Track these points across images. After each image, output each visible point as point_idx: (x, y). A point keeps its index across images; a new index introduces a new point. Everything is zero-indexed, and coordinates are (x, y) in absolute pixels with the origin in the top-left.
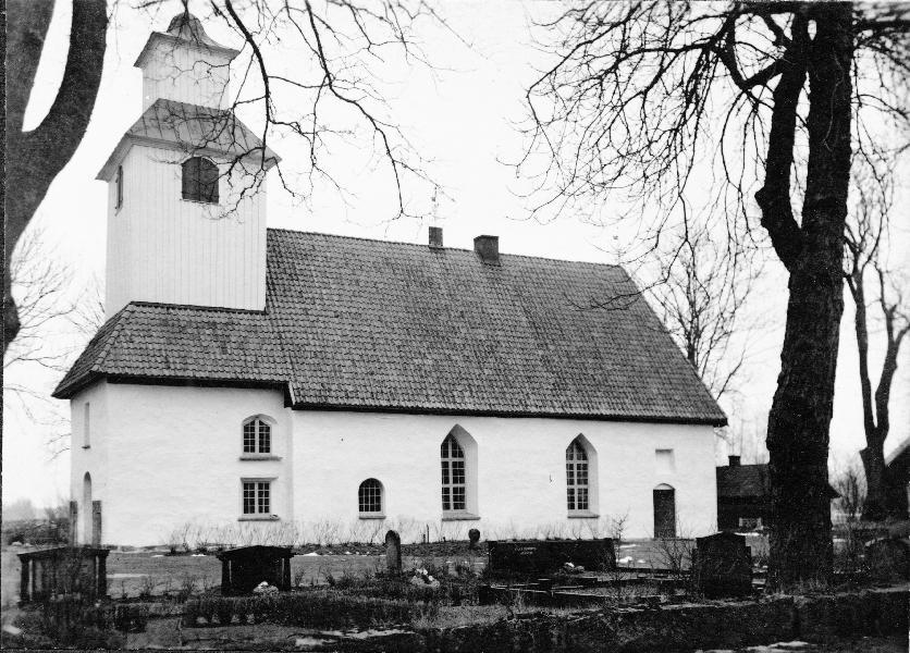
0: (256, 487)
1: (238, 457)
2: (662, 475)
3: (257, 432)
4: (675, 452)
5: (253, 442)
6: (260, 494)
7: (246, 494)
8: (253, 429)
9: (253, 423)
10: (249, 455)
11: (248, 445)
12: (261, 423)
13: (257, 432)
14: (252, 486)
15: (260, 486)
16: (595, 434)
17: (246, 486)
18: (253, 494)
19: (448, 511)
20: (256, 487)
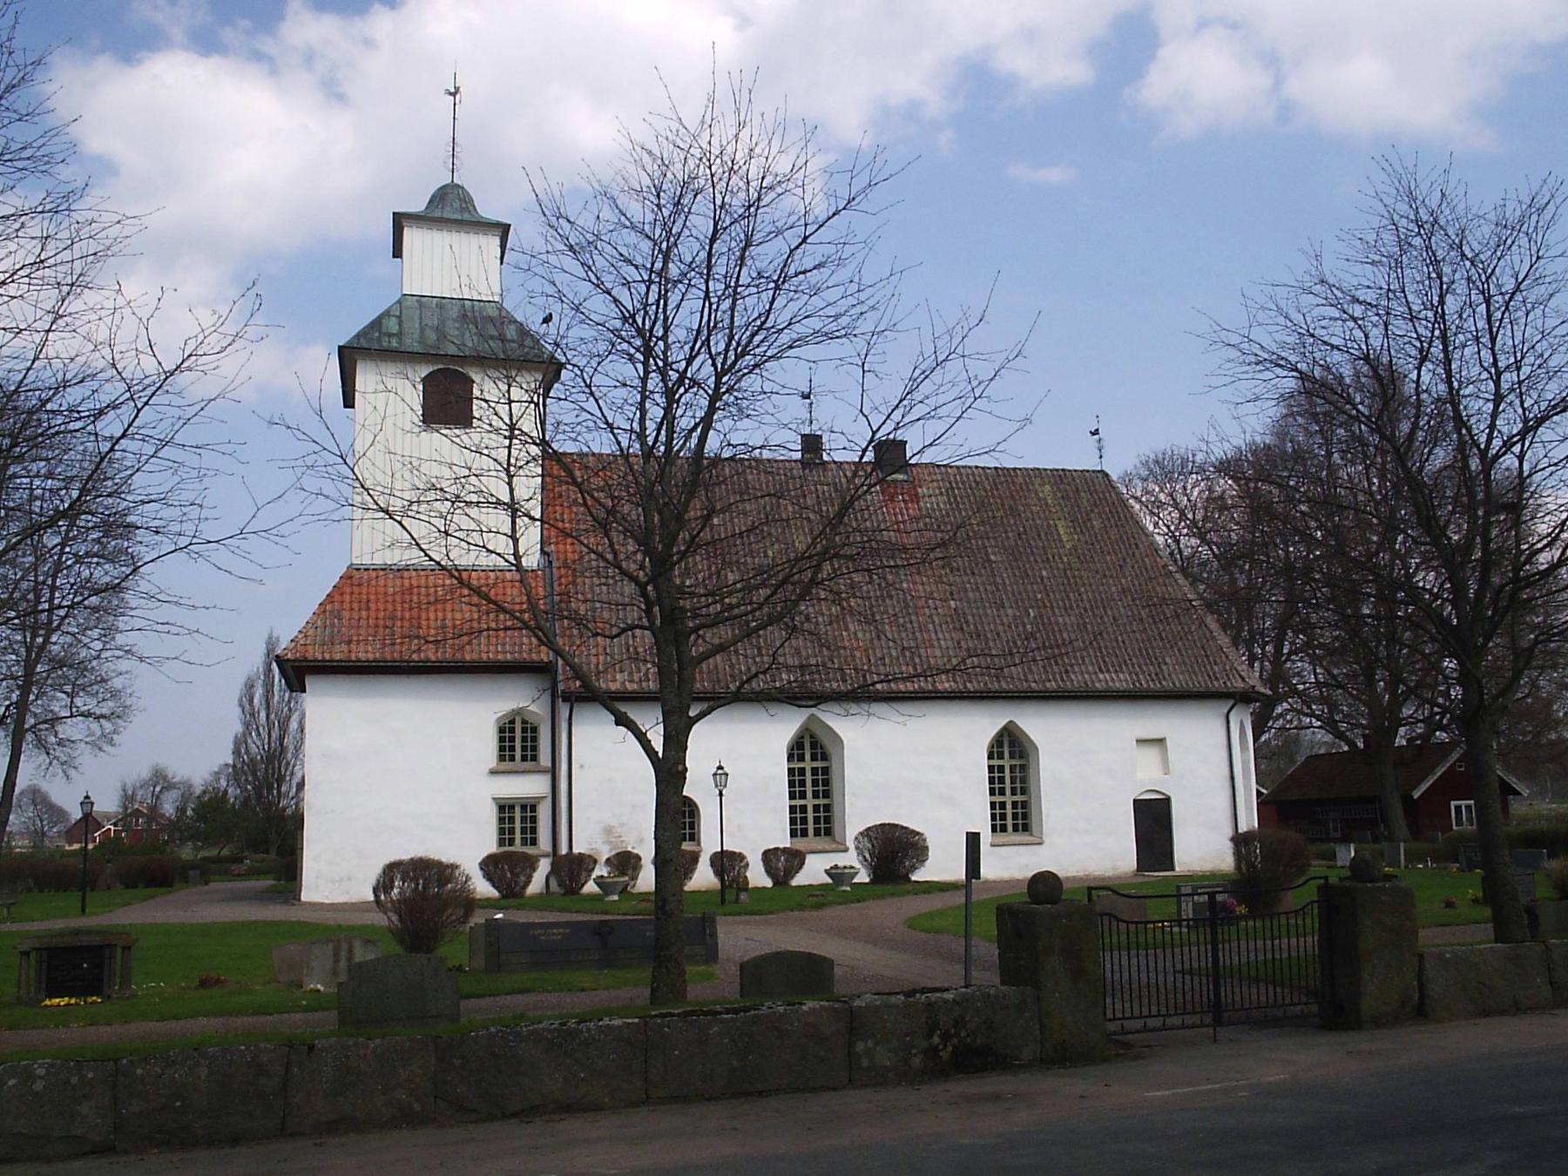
0: (518, 809)
1: (487, 771)
2: (1146, 777)
3: (518, 734)
4: (1168, 742)
5: (512, 749)
6: (523, 819)
7: (501, 820)
8: (512, 730)
9: (512, 722)
10: (507, 765)
11: (505, 749)
12: (524, 722)
13: (518, 734)
14: (512, 807)
15: (524, 807)
16: (1040, 725)
17: (501, 808)
18: (512, 820)
19: (795, 840)
20: (518, 809)
